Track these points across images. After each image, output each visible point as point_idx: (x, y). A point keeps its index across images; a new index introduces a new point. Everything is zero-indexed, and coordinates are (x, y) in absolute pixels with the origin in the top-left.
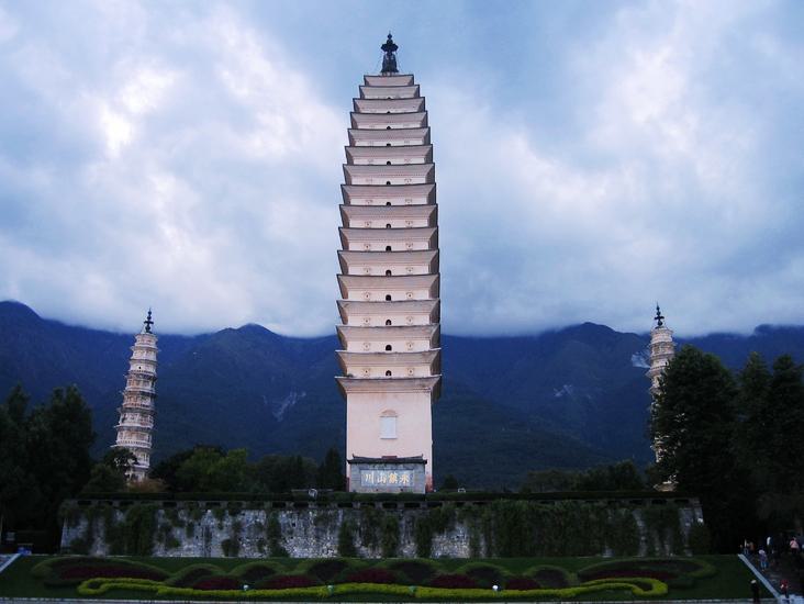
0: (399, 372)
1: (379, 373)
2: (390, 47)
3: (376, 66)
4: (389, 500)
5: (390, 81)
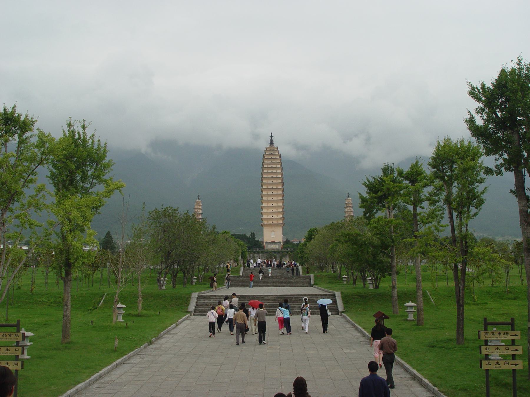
0: (275, 222)
1: (270, 222)
2: (272, 137)
3: (268, 145)
4: (275, 252)
5: (272, 149)
